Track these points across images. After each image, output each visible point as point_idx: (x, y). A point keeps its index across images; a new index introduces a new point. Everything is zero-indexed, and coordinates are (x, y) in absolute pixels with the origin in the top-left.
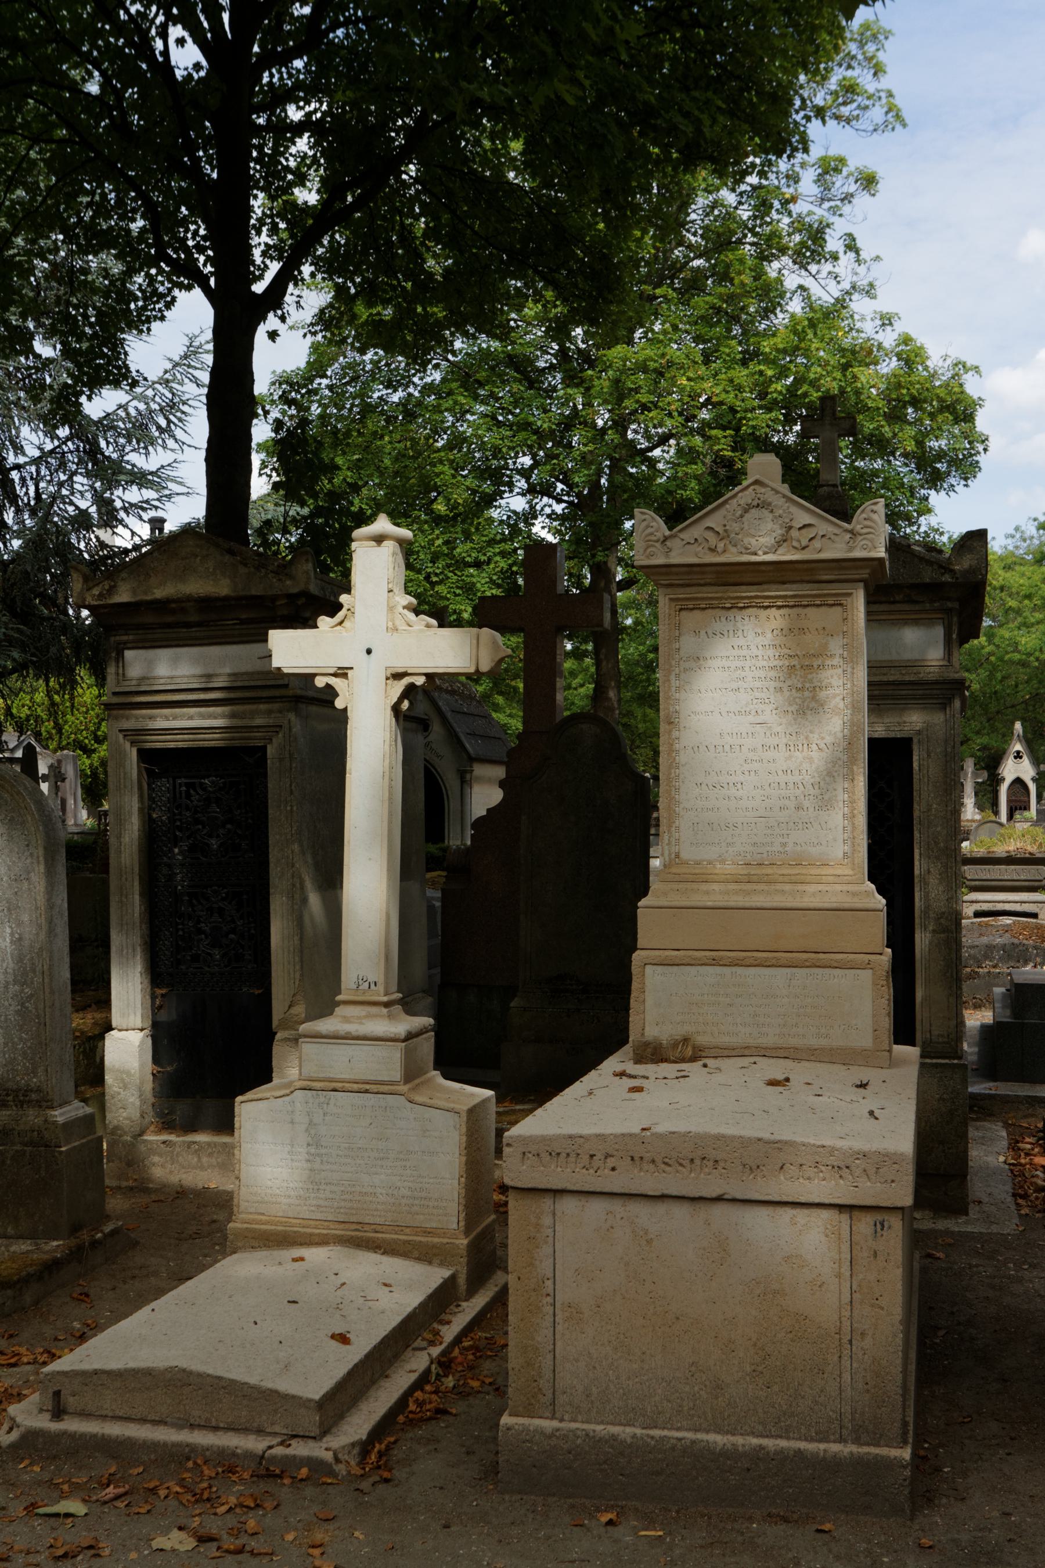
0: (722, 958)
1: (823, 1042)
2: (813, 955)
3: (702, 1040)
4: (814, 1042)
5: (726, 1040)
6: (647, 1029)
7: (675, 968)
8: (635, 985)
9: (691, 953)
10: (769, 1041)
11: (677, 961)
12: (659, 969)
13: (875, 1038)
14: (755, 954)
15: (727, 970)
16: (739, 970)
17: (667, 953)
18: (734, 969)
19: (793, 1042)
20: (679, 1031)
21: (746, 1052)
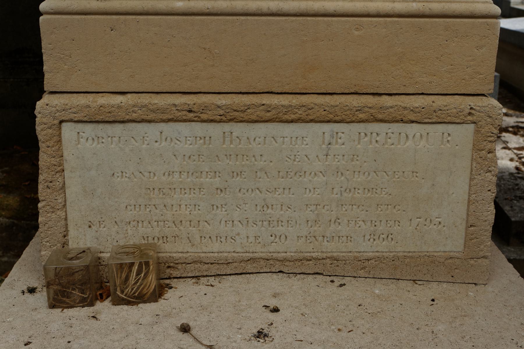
0: (205, 108)
1: (382, 247)
2: (371, 100)
3: (171, 250)
4: (366, 248)
5: (214, 249)
6: (72, 233)
7: (118, 128)
8: (44, 159)
9: (145, 99)
10: (290, 246)
11: (122, 115)
12: (89, 128)
13: (468, 238)
14: (267, 100)
15: (215, 130)
16: (238, 129)
17: (102, 100)
18: (227, 127)
19: (331, 248)
20: (134, 237)
21: (250, 268)
